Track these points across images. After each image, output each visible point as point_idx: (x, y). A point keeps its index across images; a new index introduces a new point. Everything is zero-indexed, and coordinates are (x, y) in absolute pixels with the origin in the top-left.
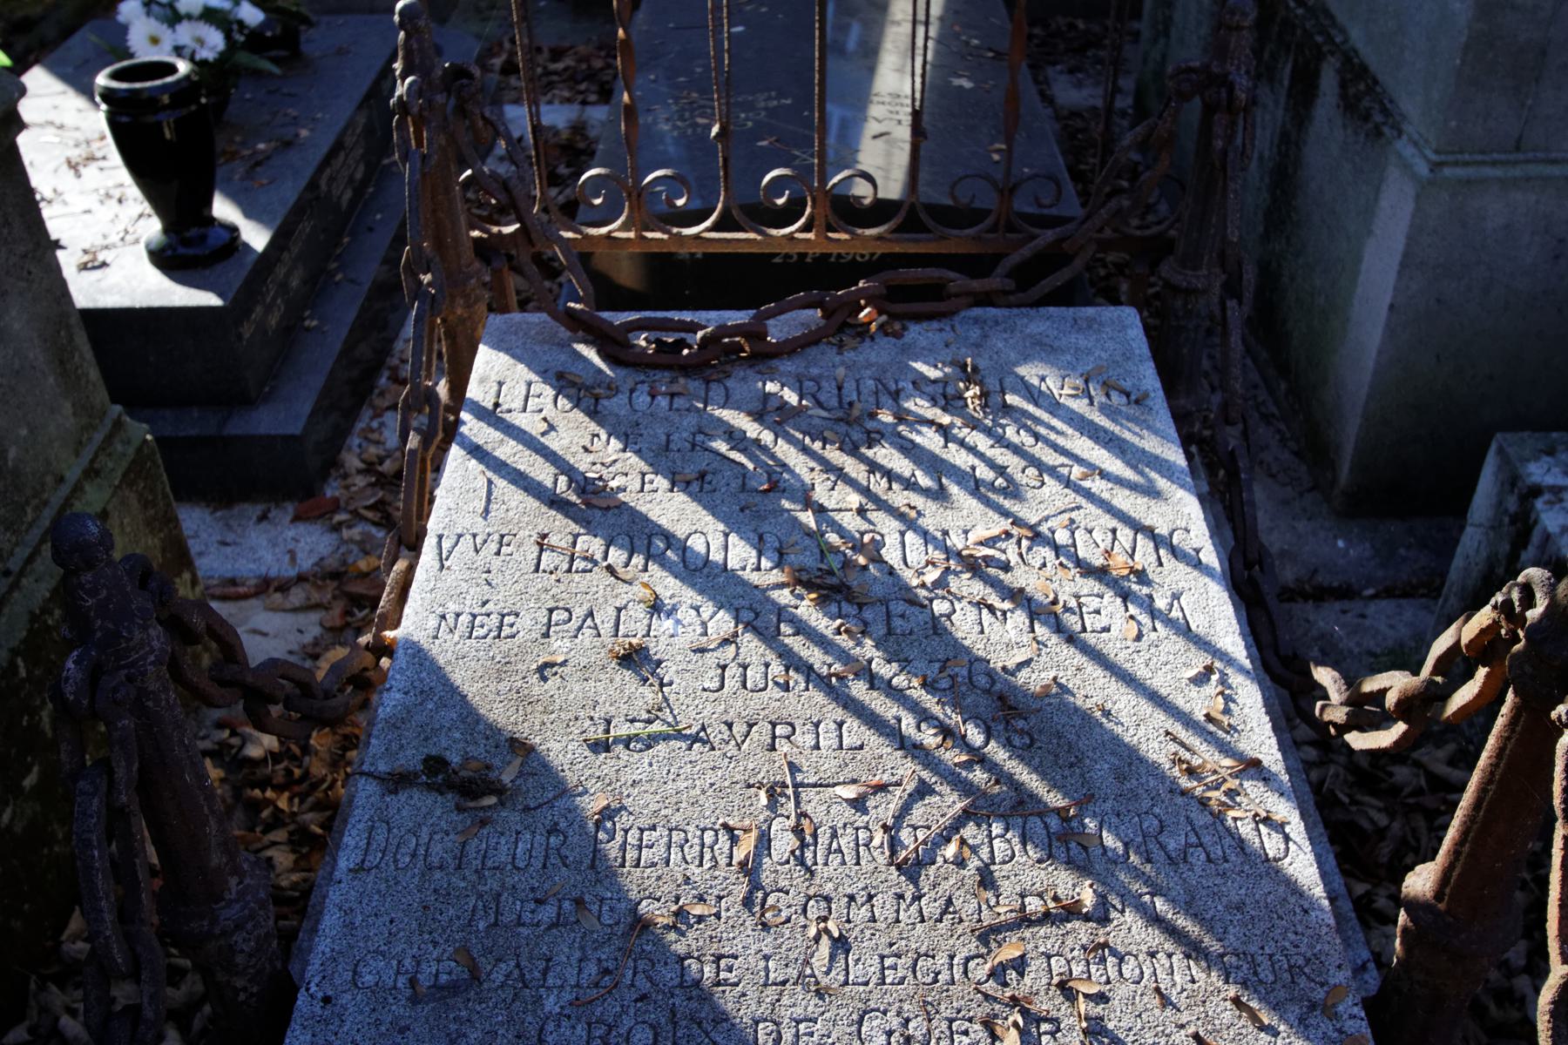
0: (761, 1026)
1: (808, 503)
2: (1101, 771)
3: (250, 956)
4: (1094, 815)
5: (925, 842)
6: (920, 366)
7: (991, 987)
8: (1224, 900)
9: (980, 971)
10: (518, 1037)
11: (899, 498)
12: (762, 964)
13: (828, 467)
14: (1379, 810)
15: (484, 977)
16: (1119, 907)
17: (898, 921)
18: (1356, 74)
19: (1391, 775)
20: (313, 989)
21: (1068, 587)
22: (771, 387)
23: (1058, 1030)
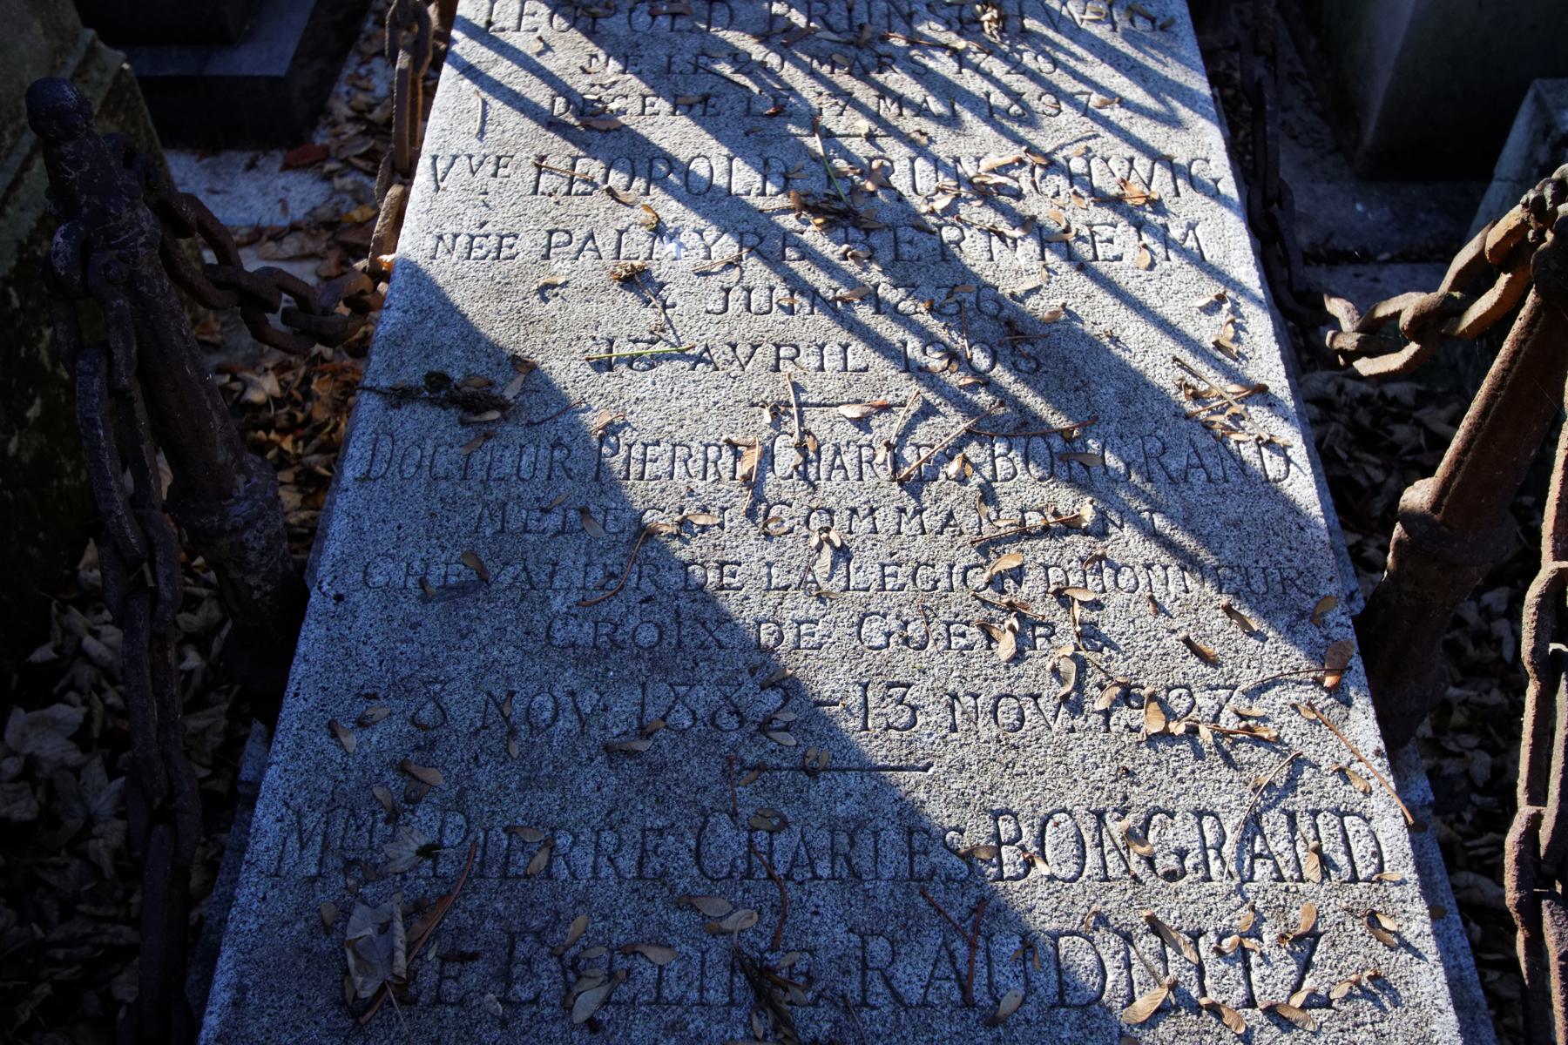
0: (763, 626)
1: (815, 127)
2: (1107, 395)
3: (262, 554)
4: (1098, 437)
5: (927, 460)
7: (988, 594)
8: (1222, 517)
9: (979, 579)
10: (528, 633)
11: (910, 124)
12: (765, 570)
13: (837, 92)
14: (1376, 467)
15: (491, 579)
16: (1118, 523)
17: (899, 532)
19: (1391, 433)
20: (325, 587)
21: (1081, 215)
23: (1053, 633)
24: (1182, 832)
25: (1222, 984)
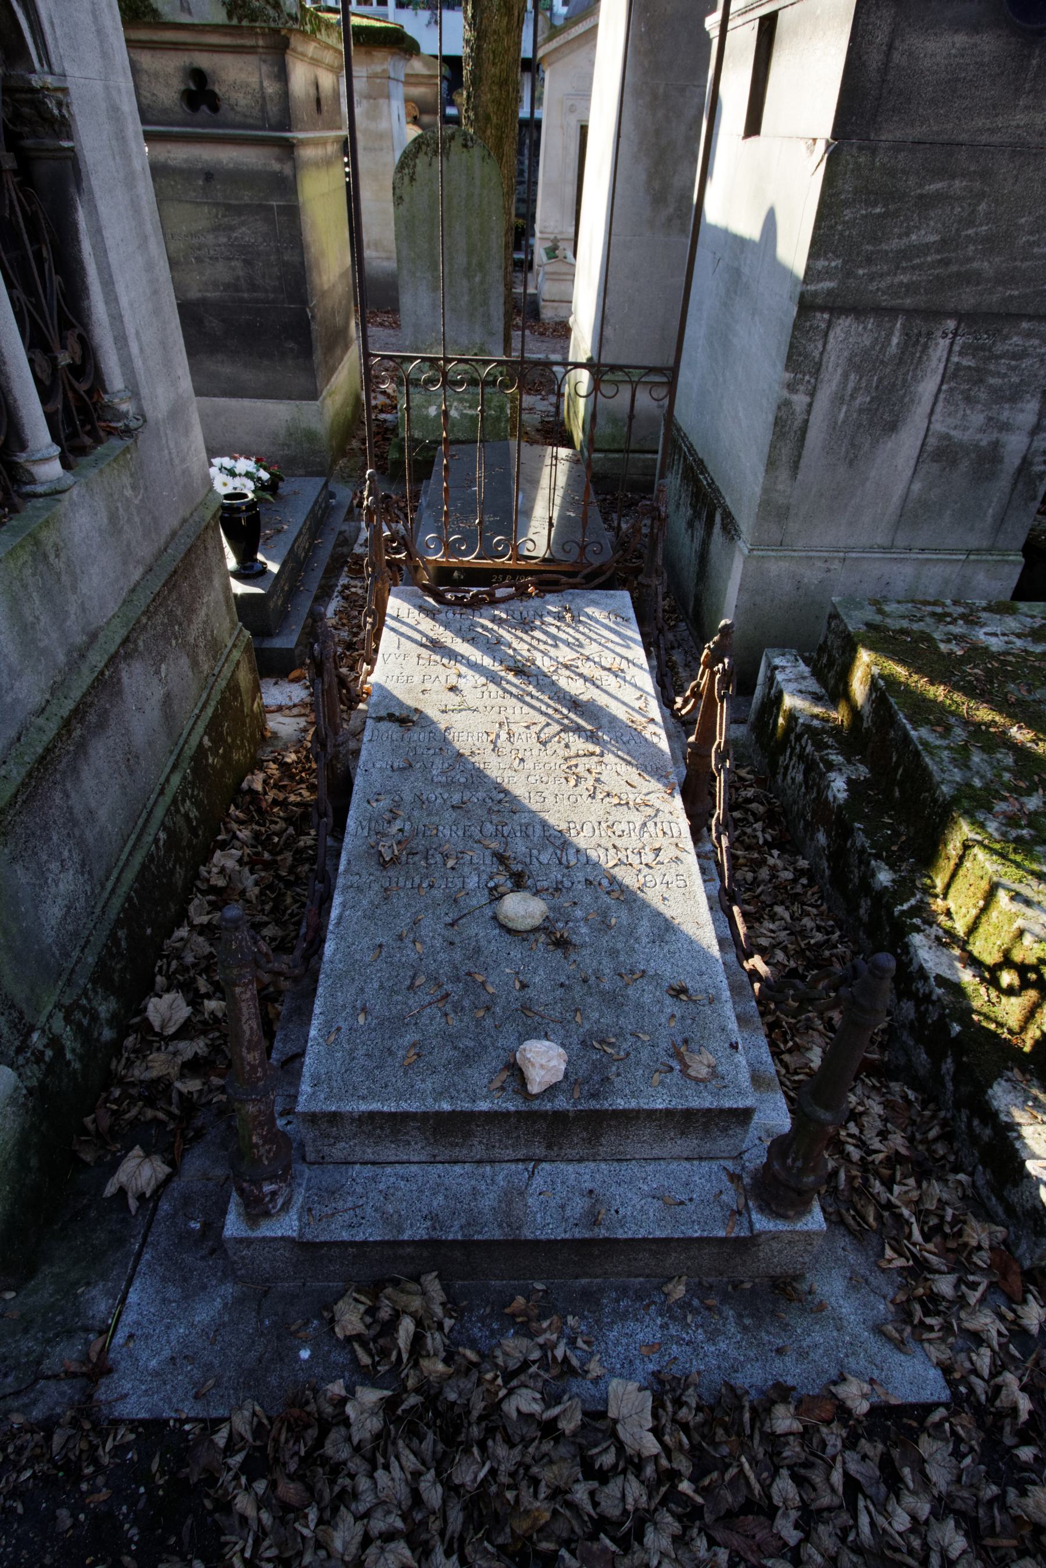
1: (510, 647)
2: (604, 721)
6: (550, 607)
9: (564, 767)
11: (542, 647)
13: (517, 637)
18: (727, 515)
21: (597, 673)
22: (497, 612)
24: (624, 826)
25: (634, 859)
